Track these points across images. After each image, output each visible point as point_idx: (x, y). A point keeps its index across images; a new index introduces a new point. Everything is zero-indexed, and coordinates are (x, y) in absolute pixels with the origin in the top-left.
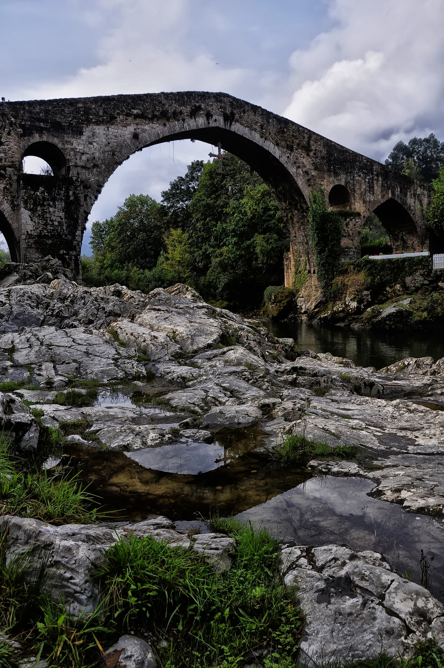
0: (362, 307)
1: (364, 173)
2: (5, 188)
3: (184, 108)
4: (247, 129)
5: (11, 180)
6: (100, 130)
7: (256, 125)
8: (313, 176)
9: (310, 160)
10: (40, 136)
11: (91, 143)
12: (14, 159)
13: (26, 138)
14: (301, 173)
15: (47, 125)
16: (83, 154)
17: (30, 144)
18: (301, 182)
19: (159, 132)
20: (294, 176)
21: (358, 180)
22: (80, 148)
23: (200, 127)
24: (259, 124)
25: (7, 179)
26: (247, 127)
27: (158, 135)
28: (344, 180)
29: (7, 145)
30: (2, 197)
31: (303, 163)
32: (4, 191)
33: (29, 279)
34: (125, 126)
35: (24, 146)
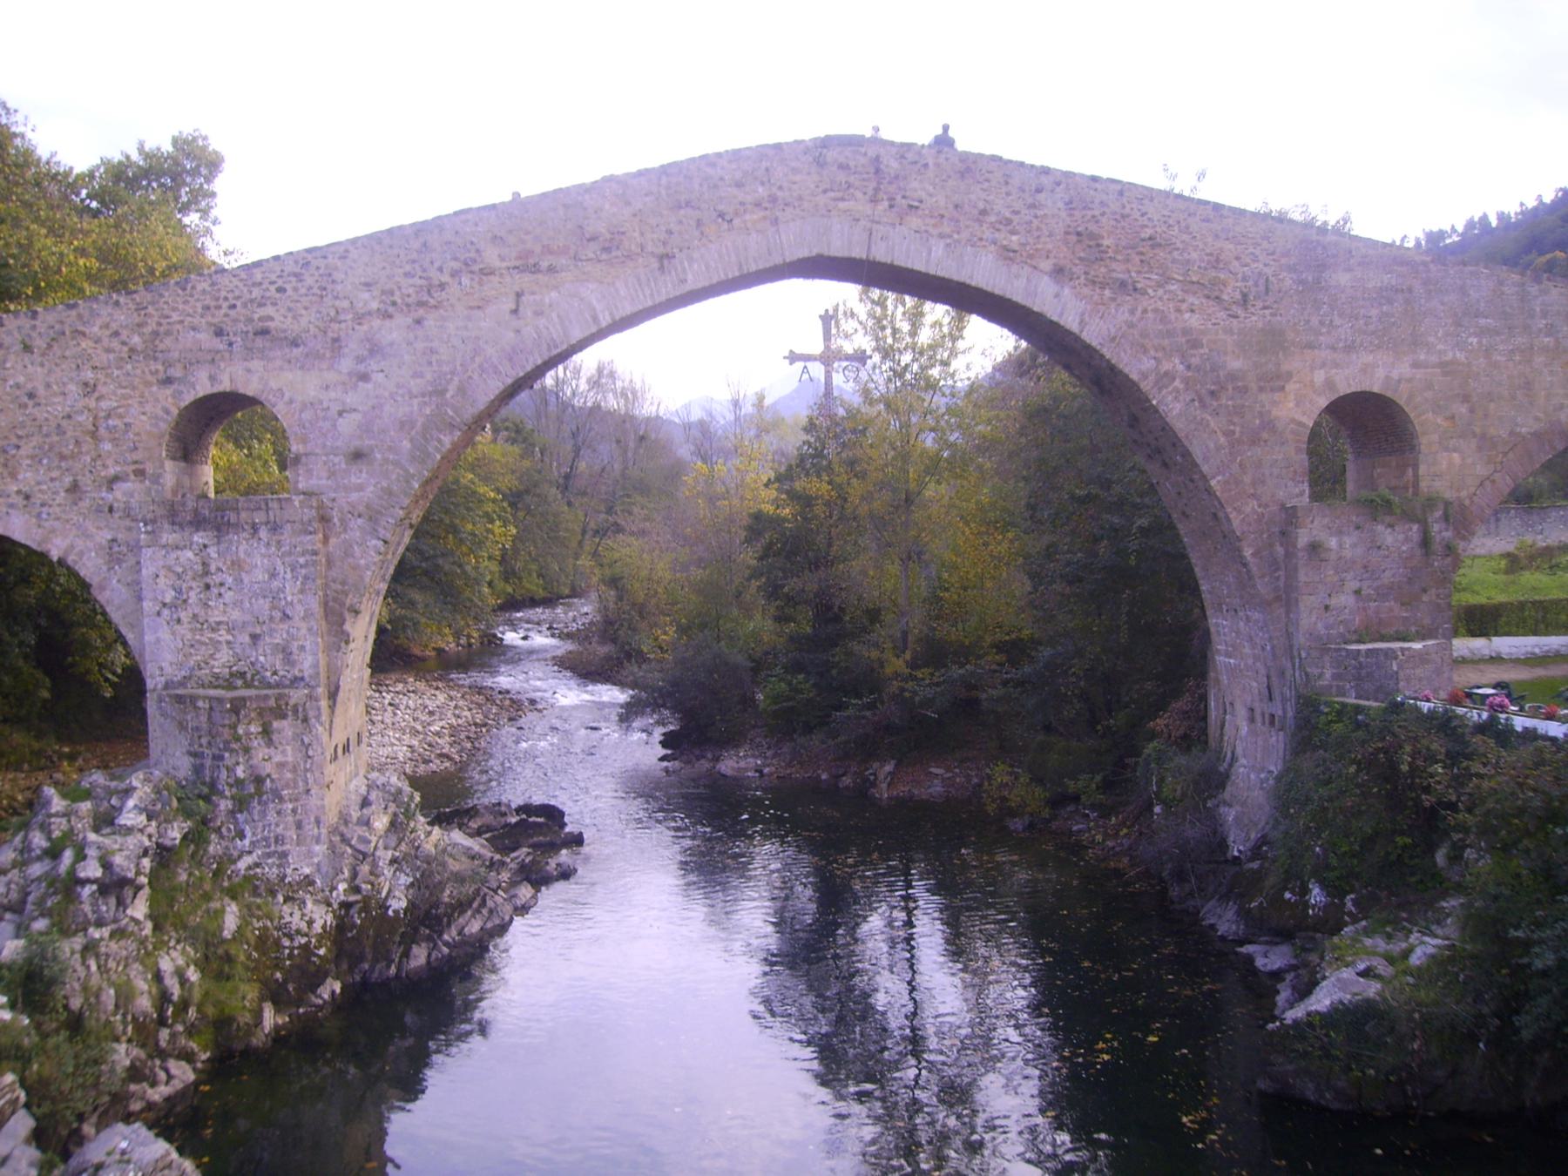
0: (1349, 905)
1: (1482, 332)
2: (114, 540)
3: (689, 211)
4: (942, 244)
5: (128, 516)
6: (393, 332)
7: (980, 222)
8: (1232, 377)
9: (1223, 314)
10: (212, 378)
11: (364, 377)
12: (138, 456)
13: (169, 391)
14: (1181, 367)
15: (231, 344)
16: (340, 414)
17: (183, 405)
18: (1173, 406)
19: (599, 307)
20: (1145, 386)
21: (1454, 362)
22: (333, 395)
23: (753, 268)
24: (993, 219)
25: (121, 514)
26: (941, 236)
27: (595, 319)
28: (1380, 373)
29: (121, 417)
30: (105, 568)
31: (1186, 331)
32: (110, 548)
33: (39, 858)
34: (479, 307)
35: (167, 412)
